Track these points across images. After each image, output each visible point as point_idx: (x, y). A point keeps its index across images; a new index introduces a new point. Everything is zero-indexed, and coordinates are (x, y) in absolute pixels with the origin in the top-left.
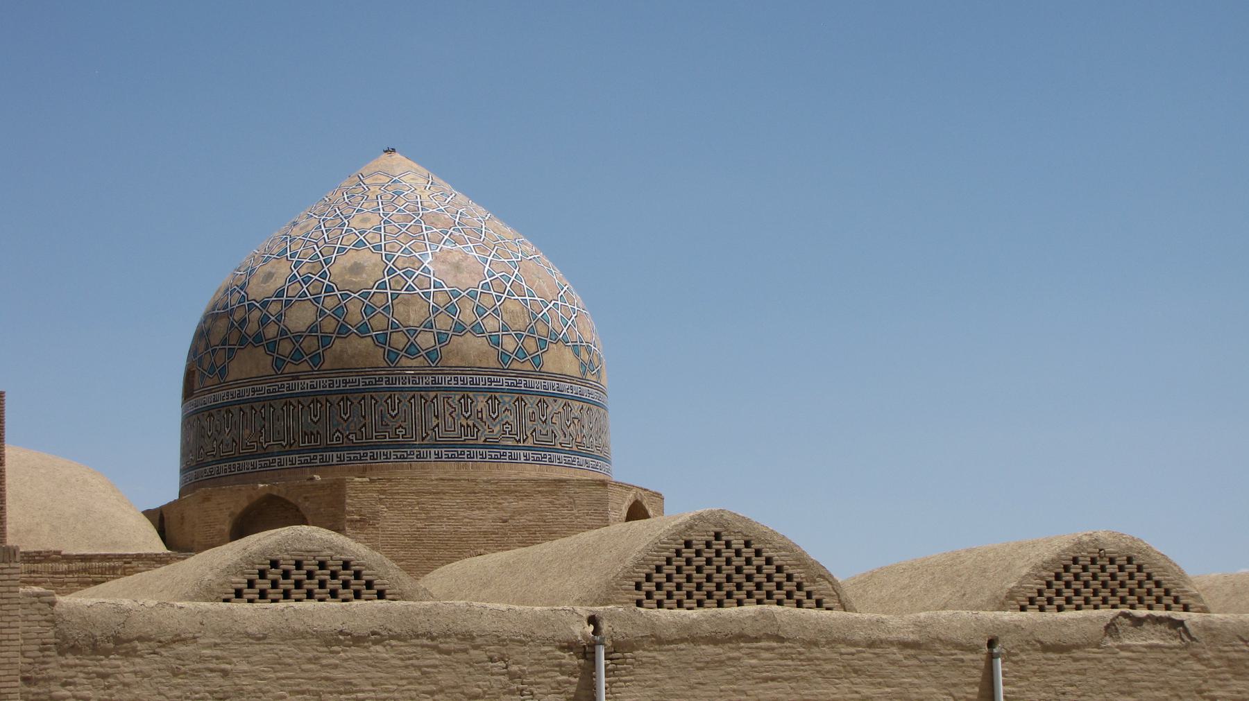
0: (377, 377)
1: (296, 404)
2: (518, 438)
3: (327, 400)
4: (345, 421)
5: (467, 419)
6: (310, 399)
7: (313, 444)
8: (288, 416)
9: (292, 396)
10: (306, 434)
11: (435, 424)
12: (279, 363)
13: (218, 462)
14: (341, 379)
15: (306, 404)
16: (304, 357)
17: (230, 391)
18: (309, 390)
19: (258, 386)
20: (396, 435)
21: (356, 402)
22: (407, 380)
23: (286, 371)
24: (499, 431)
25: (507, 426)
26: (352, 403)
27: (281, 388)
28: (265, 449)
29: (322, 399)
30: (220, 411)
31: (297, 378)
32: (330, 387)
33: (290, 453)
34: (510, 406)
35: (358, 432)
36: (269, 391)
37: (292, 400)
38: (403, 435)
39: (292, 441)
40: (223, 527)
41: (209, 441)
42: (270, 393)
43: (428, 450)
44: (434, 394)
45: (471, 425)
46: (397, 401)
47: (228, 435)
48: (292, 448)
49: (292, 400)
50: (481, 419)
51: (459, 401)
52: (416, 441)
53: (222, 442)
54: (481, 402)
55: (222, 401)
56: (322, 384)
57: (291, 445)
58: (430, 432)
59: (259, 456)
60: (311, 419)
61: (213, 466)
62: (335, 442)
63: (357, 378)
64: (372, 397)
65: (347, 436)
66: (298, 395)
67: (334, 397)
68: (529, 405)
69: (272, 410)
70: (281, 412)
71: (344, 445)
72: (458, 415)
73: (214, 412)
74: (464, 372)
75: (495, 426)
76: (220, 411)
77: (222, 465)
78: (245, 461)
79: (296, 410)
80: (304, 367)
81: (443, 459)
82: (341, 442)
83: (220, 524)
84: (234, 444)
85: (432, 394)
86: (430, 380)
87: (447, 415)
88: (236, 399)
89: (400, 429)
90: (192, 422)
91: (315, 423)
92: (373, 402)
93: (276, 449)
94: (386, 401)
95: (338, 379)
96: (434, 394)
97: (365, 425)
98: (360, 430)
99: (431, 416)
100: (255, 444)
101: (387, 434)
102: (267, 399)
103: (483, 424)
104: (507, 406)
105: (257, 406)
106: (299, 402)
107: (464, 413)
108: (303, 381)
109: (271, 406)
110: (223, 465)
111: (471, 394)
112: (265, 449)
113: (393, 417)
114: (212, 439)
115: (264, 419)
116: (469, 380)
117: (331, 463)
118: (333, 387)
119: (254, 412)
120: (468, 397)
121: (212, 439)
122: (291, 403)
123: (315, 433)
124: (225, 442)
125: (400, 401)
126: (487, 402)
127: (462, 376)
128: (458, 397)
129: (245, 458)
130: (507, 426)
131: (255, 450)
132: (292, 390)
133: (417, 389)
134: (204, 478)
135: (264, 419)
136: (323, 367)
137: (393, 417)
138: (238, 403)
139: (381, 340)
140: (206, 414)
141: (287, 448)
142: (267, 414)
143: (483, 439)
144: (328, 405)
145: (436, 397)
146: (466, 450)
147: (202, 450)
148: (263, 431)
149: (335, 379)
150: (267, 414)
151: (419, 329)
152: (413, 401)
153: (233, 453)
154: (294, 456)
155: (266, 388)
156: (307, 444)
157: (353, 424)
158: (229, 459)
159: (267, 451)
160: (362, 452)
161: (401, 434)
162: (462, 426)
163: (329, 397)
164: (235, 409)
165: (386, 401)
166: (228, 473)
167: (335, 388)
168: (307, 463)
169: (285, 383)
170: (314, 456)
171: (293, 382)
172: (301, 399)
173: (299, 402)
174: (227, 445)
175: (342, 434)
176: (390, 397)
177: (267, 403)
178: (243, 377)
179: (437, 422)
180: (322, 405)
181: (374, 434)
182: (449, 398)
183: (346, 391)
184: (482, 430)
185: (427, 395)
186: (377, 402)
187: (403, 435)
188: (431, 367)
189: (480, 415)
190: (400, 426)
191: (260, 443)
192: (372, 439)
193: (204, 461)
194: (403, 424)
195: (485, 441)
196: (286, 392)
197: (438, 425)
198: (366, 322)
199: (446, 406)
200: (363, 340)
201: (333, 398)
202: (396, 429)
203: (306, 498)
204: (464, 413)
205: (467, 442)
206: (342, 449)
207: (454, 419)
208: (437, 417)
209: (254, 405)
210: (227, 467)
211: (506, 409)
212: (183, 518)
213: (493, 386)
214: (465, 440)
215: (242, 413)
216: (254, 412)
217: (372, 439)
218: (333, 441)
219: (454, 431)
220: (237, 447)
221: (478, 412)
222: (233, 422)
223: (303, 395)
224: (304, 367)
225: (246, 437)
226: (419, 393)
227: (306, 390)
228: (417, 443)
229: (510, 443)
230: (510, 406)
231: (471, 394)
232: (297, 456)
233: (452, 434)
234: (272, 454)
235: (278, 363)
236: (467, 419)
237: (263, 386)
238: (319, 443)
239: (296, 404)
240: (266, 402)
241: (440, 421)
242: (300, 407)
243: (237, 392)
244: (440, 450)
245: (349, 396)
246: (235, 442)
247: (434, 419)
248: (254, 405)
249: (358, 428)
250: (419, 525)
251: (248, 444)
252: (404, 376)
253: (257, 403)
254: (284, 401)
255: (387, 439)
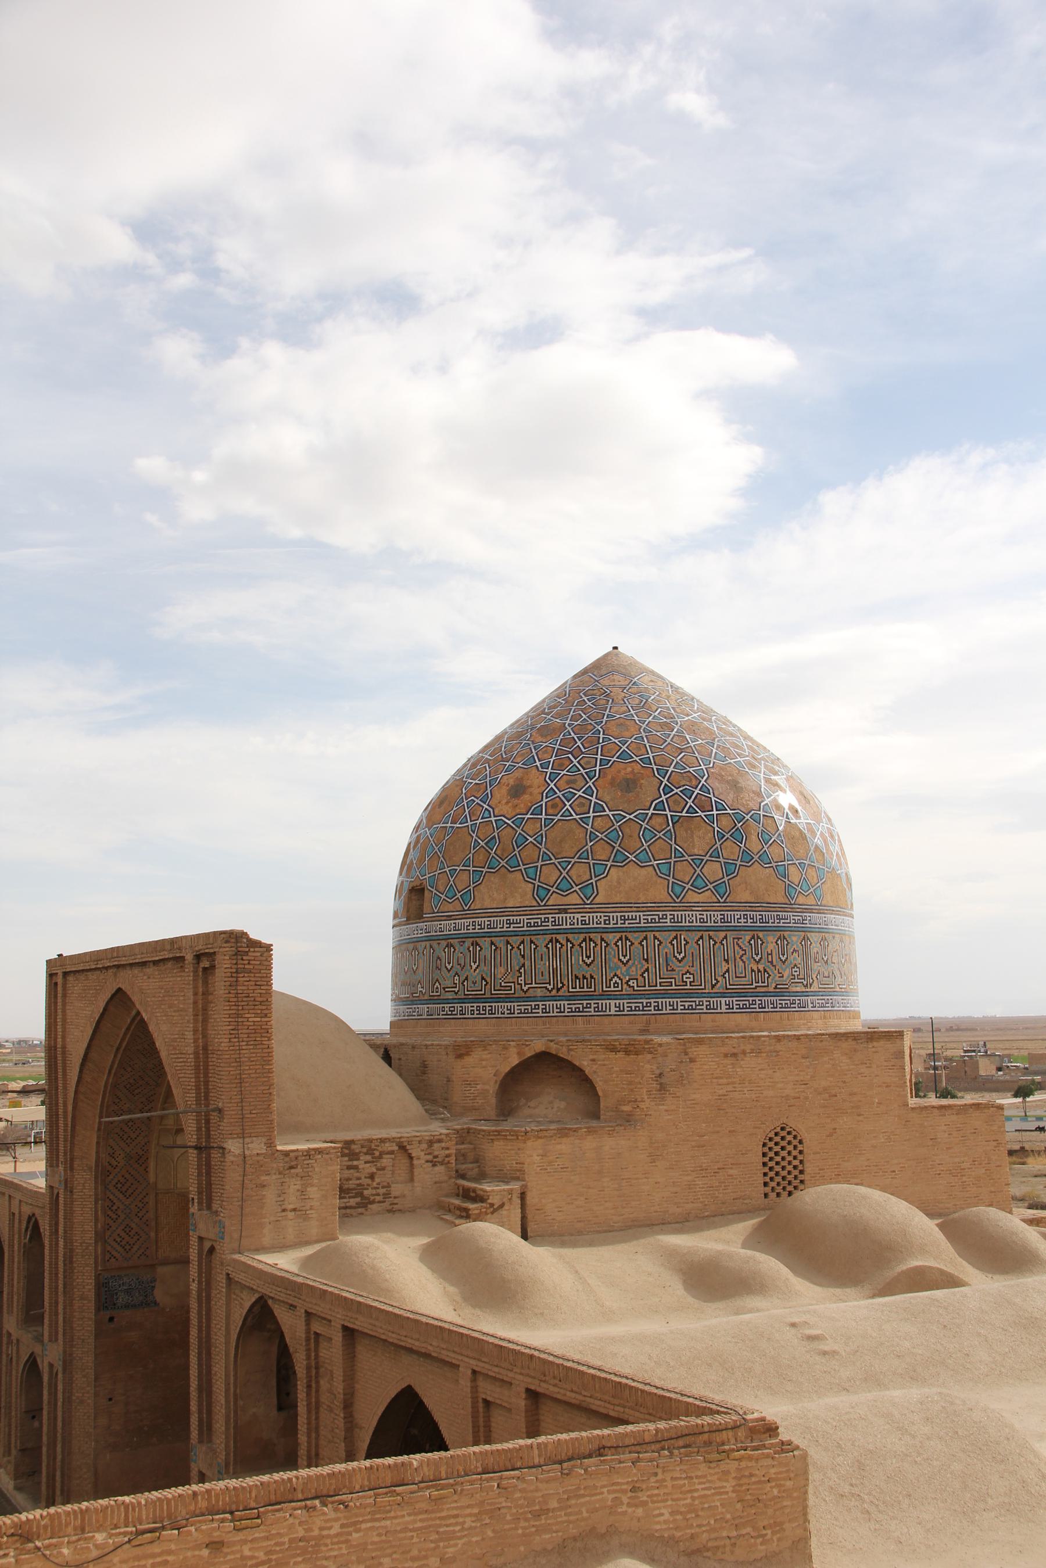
0: (660, 913)
1: (564, 942)
2: (805, 983)
3: (602, 939)
4: (625, 964)
5: (758, 963)
6: (582, 936)
7: (585, 989)
8: (555, 955)
9: (558, 932)
10: (577, 977)
11: (724, 969)
12: (542, 893)
13: (462, 1001)
14: (619, 914)
15: (576, 943)
16: (573, 887)
17: (477, 920)
18: (580, 926)
19: (515, 918)
20: (683, 981)
21: (636, 943)
22: (694, 918)
23: (550, 902)
24: (788, 977)
25: (796, 969)
26: (632, 944)
27: (545, 922)
28: (525, 992)
29: (597, 937)
30: (464, 942)
31: (565, 911)
32: (605, 924)
33: (558, 998)
34: (797, 946)
35: (640, 979)
36: (529, 925)
37: (560, 937)
38: (690, 982)
39: (560, 985)
40: (487, 1087)
41: (448, 975)
42: (531, 926)
43: (719, 999)
44: (723, 934)
45: (762, 970)
46: (683, 942)
47: (475, 970)
48: (560, 993)
49: (560, 937)
50: (772, 962)
51: (749, 942)
52: (705, 989)
53: (467, 979)
54: (770, 943)
55: (466, 931)
56: (596, 920)
57: (558, 990)
58: (719, 979)
59: (518, 999)
60: (583, 961)
61: (456, 1005)
62: (612, 989)
63: (638, 914)
64: (655, 938)
65: (627, 983)
66: (565, 932)
67: (611, 936)
68: (813, 945)
69: (533, 946)
70: (545, 949)
71: (624, 992)
72: (748, 959)
73: (455, 942)
74: (754, 909)
75: (785, 970)
76: (464, 942)
77: (467, 1005)
78: (500, 1004)
79: (564, 948)
80: (574, 899)
81: (735, 1010)
82: (620, 989)
83: (484, 1084)
84: (484, 983)
85: (722, 934)
86: (719, 919)
87: (738, 960)
88: (486, 930)
89: (688, 975)
90: (421, 949)
91: (589, 965)
92: (657, 942)
93: (539, 993)
94: (671, 943)
95: (615, 914)
96: (723, 934)
97: (647, 970)
98: (642, 975)
99: (719, 959)
100: (512, 984)
101: (673, 980)
102: (527, 933)
103: (773, 968)
104: (795, 946)
105: (515, 941)
106: (568, 940)
107: (754, 956)
108: (572, 915)
109: (532, 942)
110: (469, 1005)
111: (761, 934)
112: (525, 992)
113: (680, 961)
114: (452, 973)
115: (523, 956)
116: (758, 917)
117: (608, 1013)
118: (609, 924)
119: (510, 947)
120: (758, 937)
121: (452, 973)
122: (557, 941)
123: (588, 976)
124: (470, 979)
125: (687, 943)
126: (776, 942)
127: (752, 913)
128: (748, 938)
129: (498, 999)
130: (796, 969)
131: (513, 992)
132: (559, 925)
133: (705, 929)
134: (441, 1017)
135: (523, 956)
136: (597, 900)
137: (680, 961)
138: (489, 935)
139: (665, 870)
140: (444, 943)
141: (554, 992)
142: (527, 952)
143: (774, 985)
144: (604, 944)
145: (726, 937)
146: (757, 999)
147: (437, 984)
148: (522, 970)
149: (611, 915)
150: (527, 952)
151: (705, 859)
152: (700, 942)
153: (483, 992)
154: (562, 1003)
155: (526, 921)
156: (578, 989)
157: (634, 969)
158: (476, 999)
159: (527, 995)
160: (645, 1001)
161: (688, 980)
162: (752, 970)
163: (604, 935)
164: (485, 943)
165: (671, 943)
166: (475, 1016)
167: (611, 926)
168: (579, 1012)
169: (550, 916)
170: (587, 1004)
171: (560, 916)
172: (570, 937)
173: (568, 940)
174: (474, 983)
175: (621, 980)
176: (676, 937)
177: (527, 939)
178: (495, 906)
179: (727, 966)
180: (596, 945)
181: (659, 981)
182: (739, 939)
183: (624, 930)
184: (772, 975)
185: (716, 936)
186: (661, 943)
187: (690, 982)
188: (719, 902)
189: (770, 956)
190: (688, 972)
191: (518, 984)
192: (656, 986)
193: (441, 997)
194: (692, 970)
195: (776, 988)
196: (551, 927)
197: (728, 971)
198: (645, 849)
199: (736, 947)
200: (643, 869)
201: (612, 938)
202: (683, 975)
203: (593, 1060)
204: (754, 956)
205: (758, 990)
206: (622, 997)
207: (744, 962)
208: (727, 961)
209: (510, 939)
210: (475, 1008)
211: (794, 950)
212: (425, 1066)
213: (781, 925)
214: (756, 987)
215: (493, 948)
216: (510, 947)
217: (656, 986)
218: (610, 987)
219: (745, 977)
220: (488, 986)
221: (768, 954)
222: (482, 957)
223: (573, 931)
224: (574, 899)
225: (499, 976)
226: (707, 933)
227: (576, 926)
228: (707, 991)
229: (798, 989)
230: (797, 946)
231: (761, 934)
232: (566, 1003)
233: (743, 981)
234: (534, 999)
235: (541, 892)
236: (758, 963)
237: (522, 917)
238: (593, 989)
239: (564, 942)
240: (525, 937)
241: (730, 966)
242: (570, 945)
243: (487, 923)
244: (731, 999)
245: (629, 935)
246: (486, 981)
247: (724, 963)
248: (510, 939)
249: (640, 973)
250: (721, 1092)
251: (503, 984)
252: (690, 913)
253: (514, 938)
254: (548, 937)
255: (674, 987)
